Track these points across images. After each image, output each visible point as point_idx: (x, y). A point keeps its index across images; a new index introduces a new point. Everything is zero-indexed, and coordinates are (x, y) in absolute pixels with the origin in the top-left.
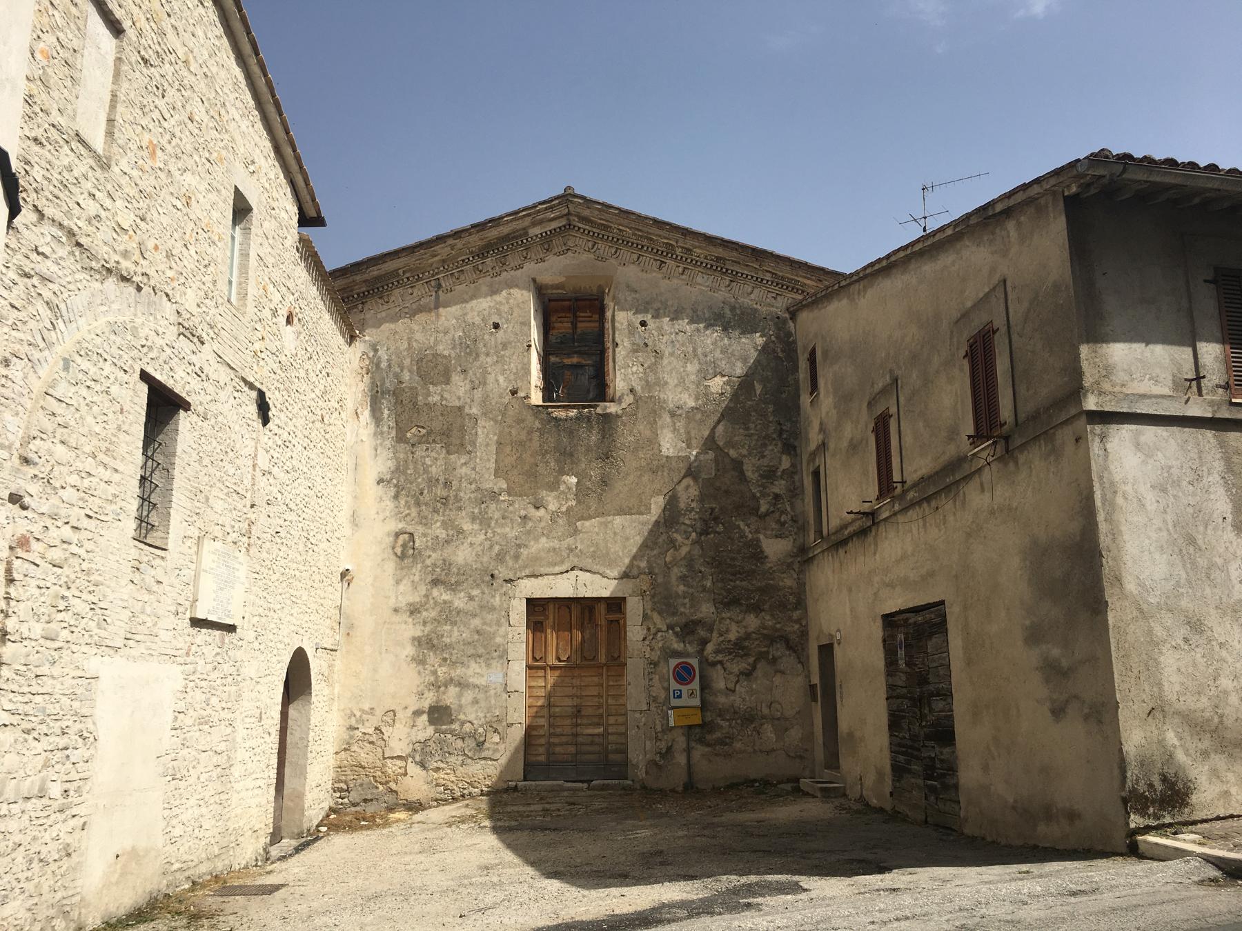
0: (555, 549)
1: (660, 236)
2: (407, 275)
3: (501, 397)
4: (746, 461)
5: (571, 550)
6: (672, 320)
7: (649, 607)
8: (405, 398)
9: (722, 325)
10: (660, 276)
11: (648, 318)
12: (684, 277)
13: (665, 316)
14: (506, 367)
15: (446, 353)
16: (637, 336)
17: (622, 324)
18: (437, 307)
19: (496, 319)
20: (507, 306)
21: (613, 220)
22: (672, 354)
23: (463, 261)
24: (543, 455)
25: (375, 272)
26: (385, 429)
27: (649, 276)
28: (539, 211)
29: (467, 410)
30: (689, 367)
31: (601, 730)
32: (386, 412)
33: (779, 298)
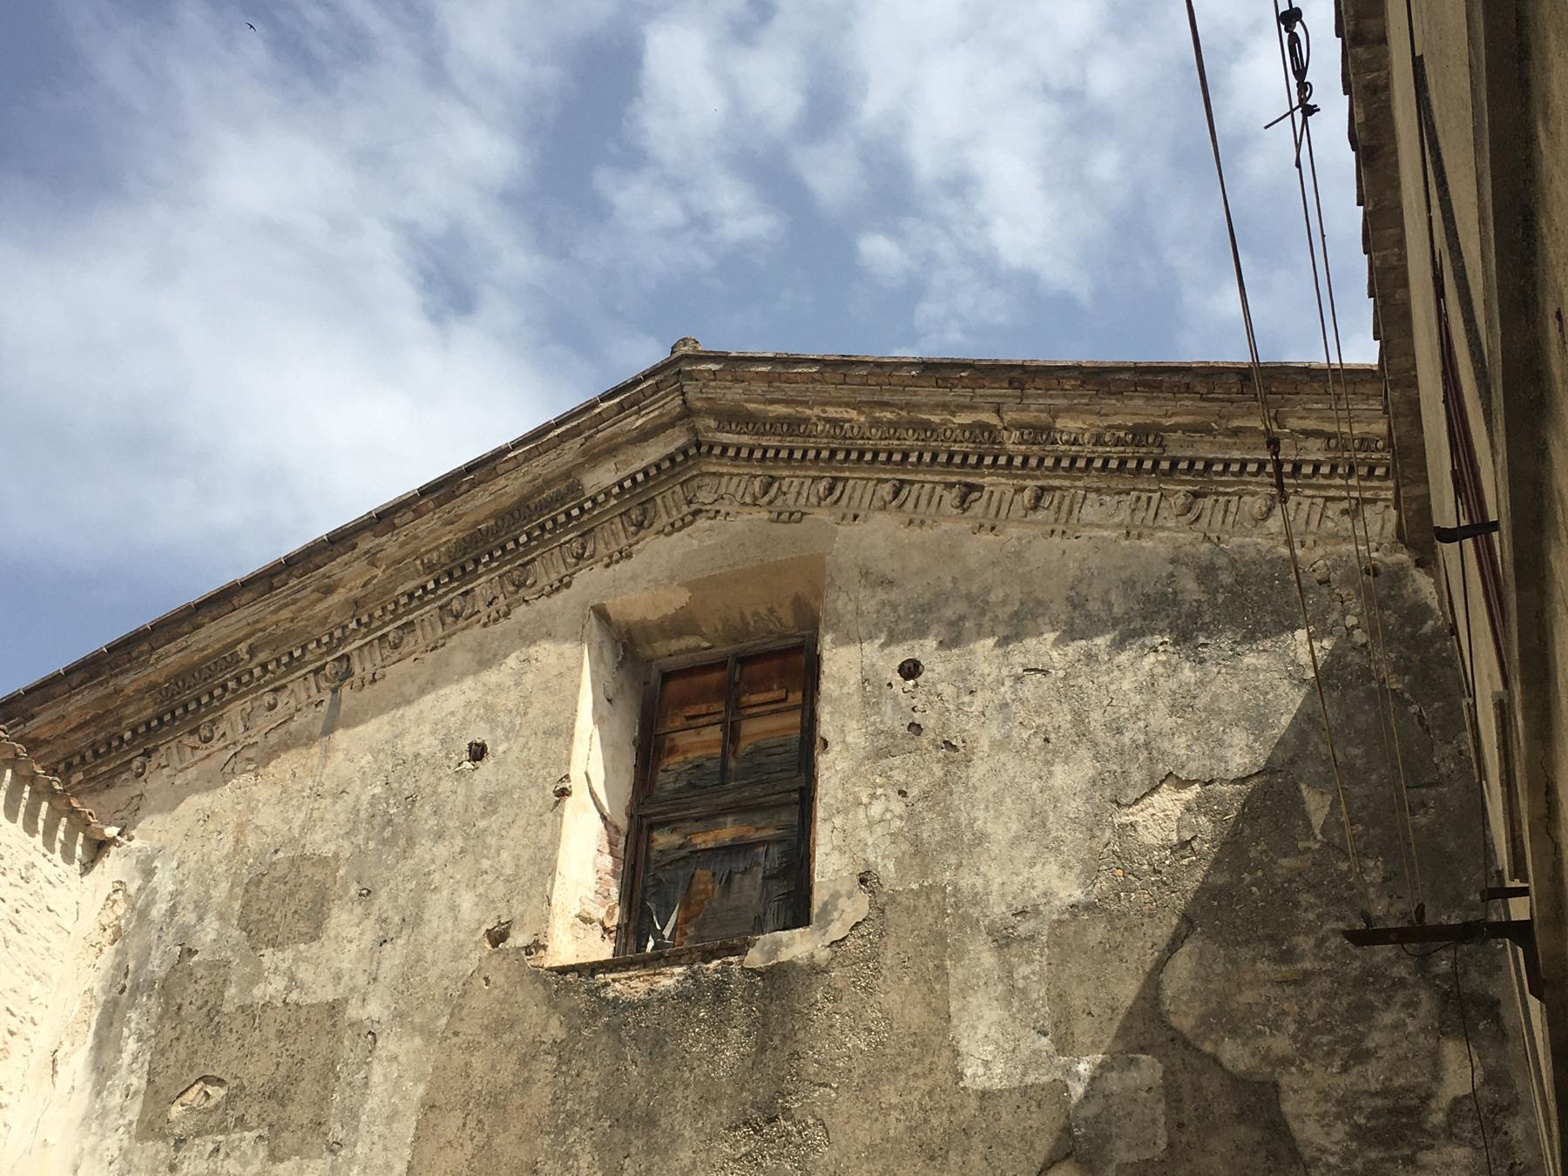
1: (945, 406)
2: (262, 657)
3: (456, 958)
4: (1289, 1079)
6: (1004, 642)
8: (191, 997)
9: (1172, 628)
10: (965, 525)
11: (926, 650)
12: (1040, 515)
13: (980, 634)
14: (486, 864)
15: (328, 850)
16: (887, 708)
17: (843, 682)
18: (328, 730)
19: (479, 734)
20: (514, 694)
21: (810, 396)
22: (1001, 745)
23: (411, 596)
24: (561, 1130)
25: (172, 657)
26: (116, 1099)
27: (928, 533)
28: (601, 418)
29: (353, 1012)
30: (1061, 775)
32: (131, 1046)
33: (1369, 511)
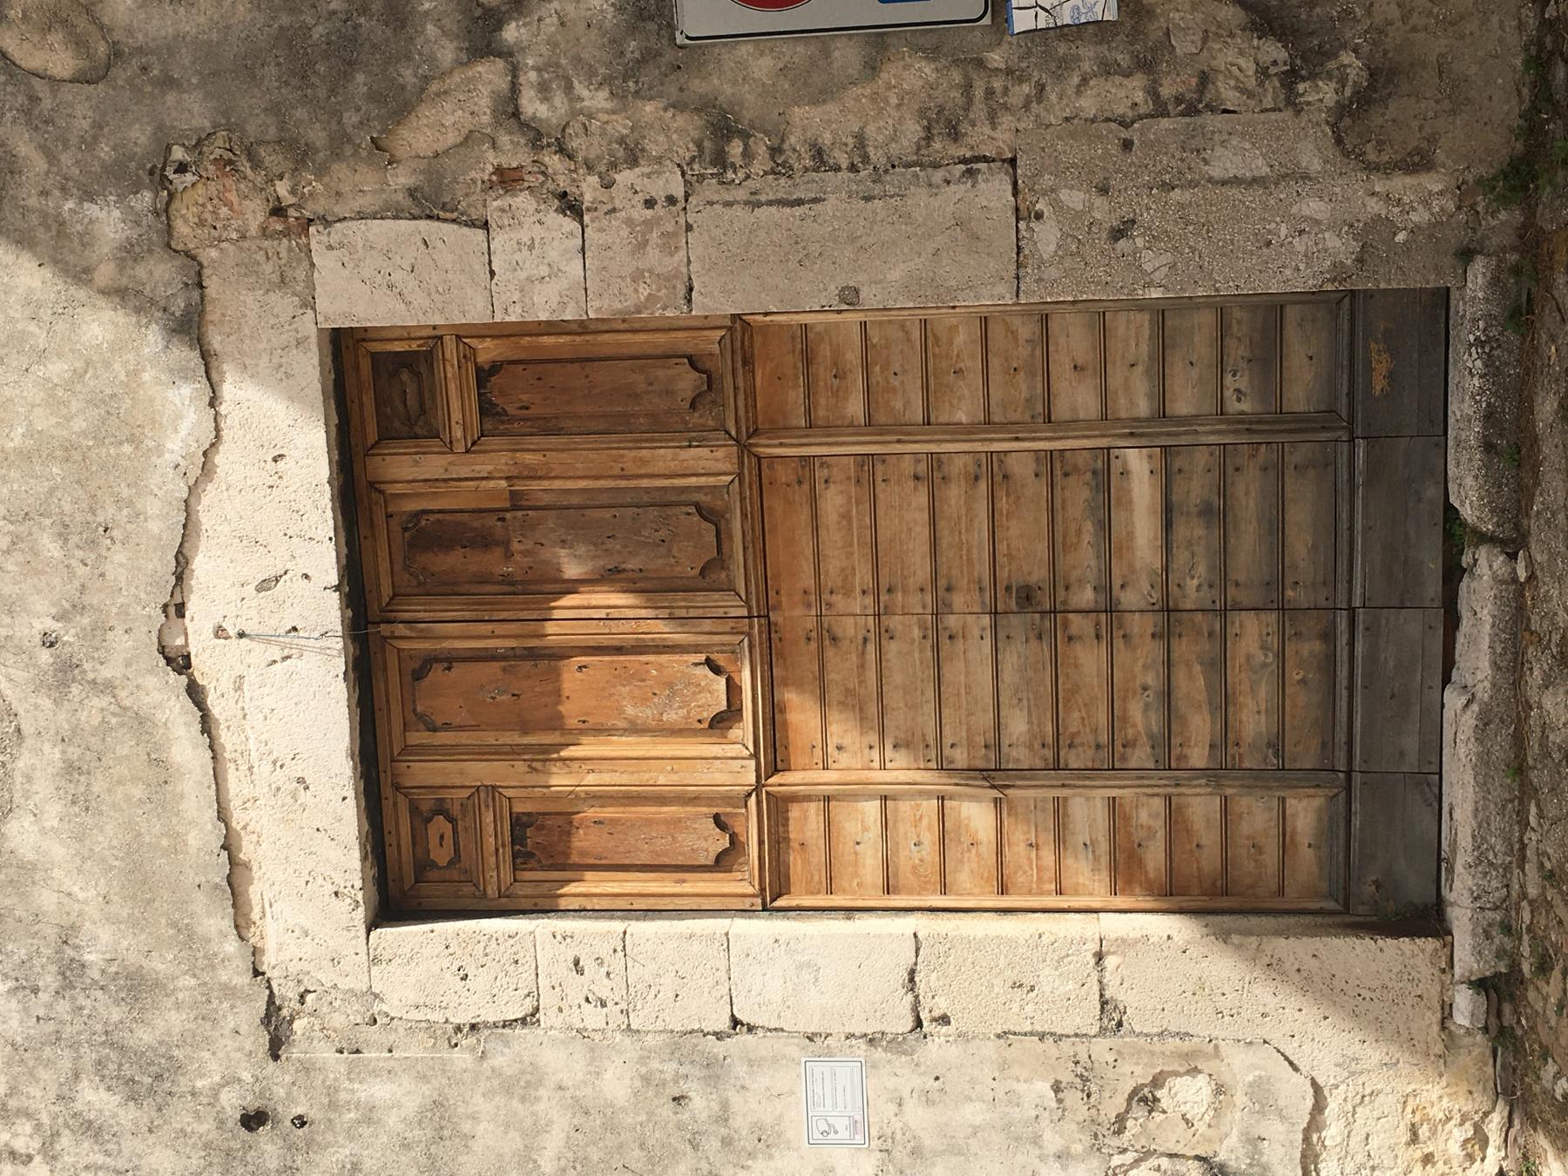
0: (71, 769)
5: (67, 671)
7: (367, 178)
31: (1138, 463)
